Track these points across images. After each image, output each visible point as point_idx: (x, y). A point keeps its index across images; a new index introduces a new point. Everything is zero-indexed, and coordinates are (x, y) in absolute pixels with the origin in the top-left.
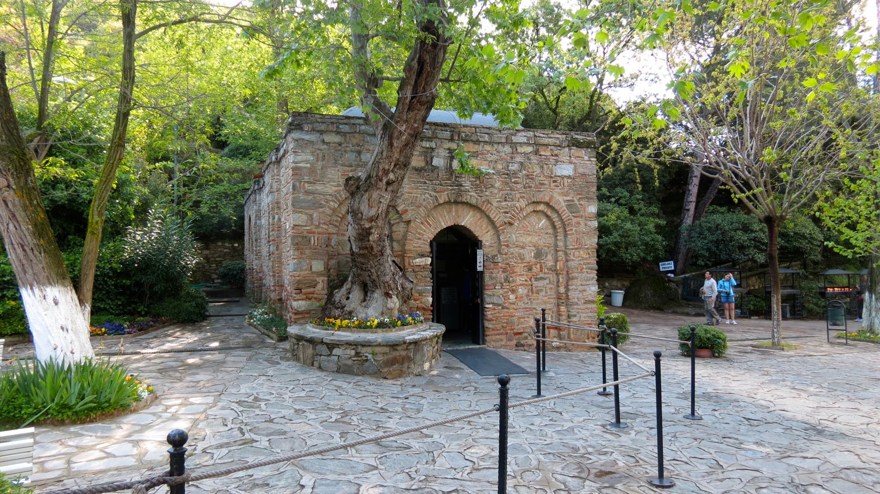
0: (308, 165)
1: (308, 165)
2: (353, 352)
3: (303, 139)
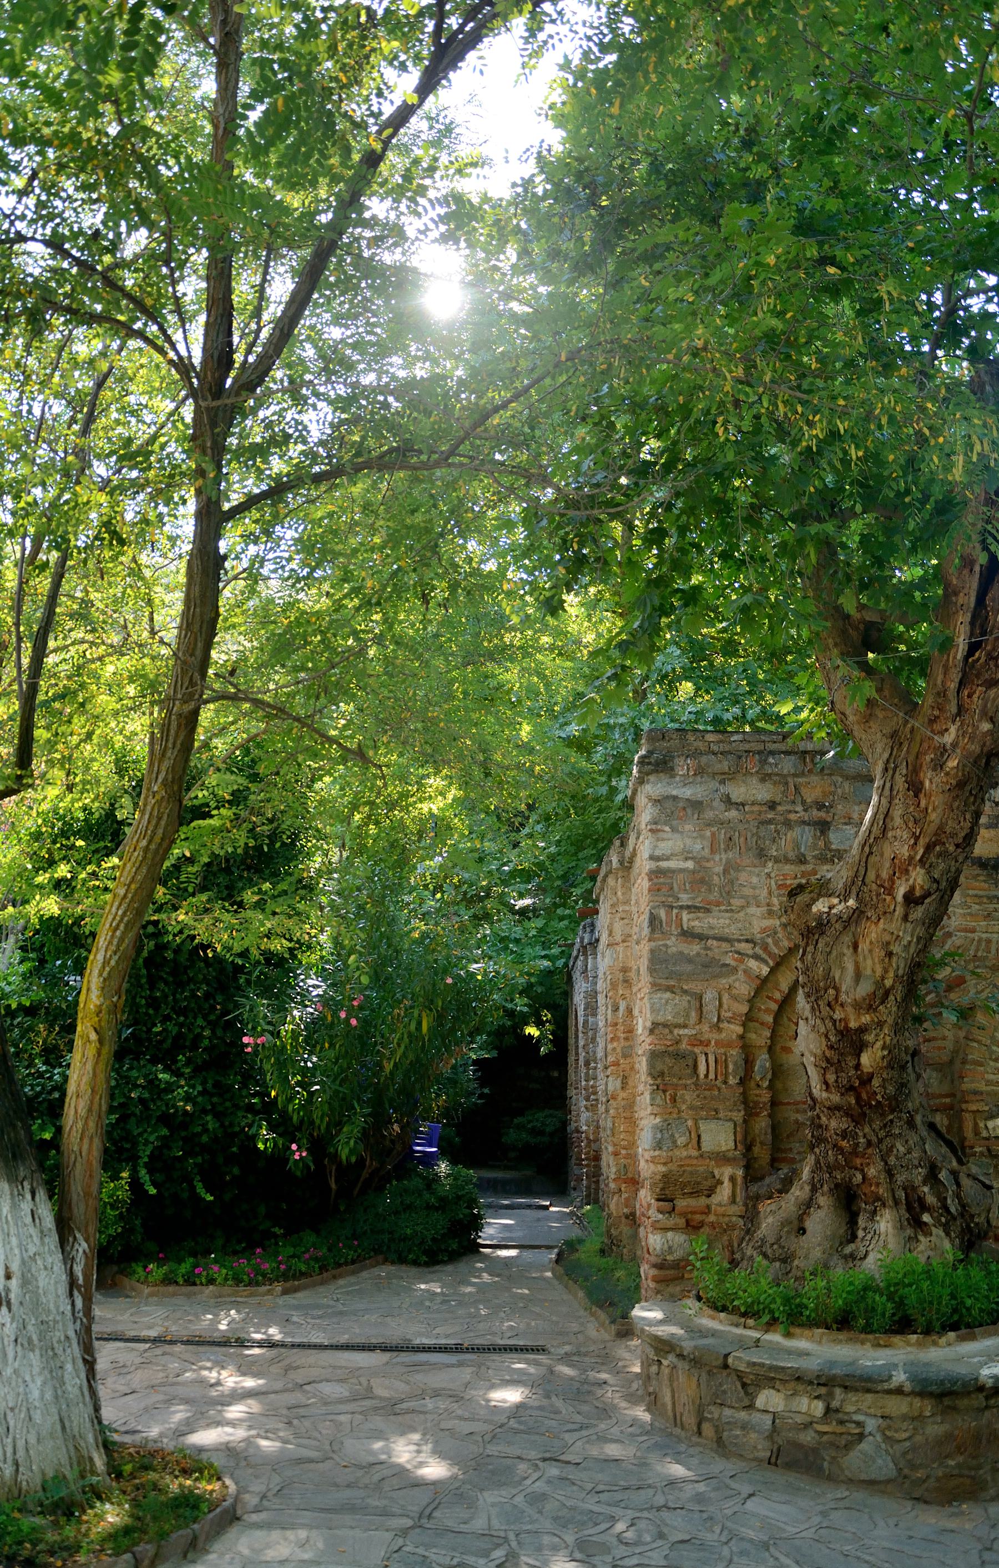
0: (690, 865)
1: (690, 865)
2: (818, 1408)
3: (675, 798)
